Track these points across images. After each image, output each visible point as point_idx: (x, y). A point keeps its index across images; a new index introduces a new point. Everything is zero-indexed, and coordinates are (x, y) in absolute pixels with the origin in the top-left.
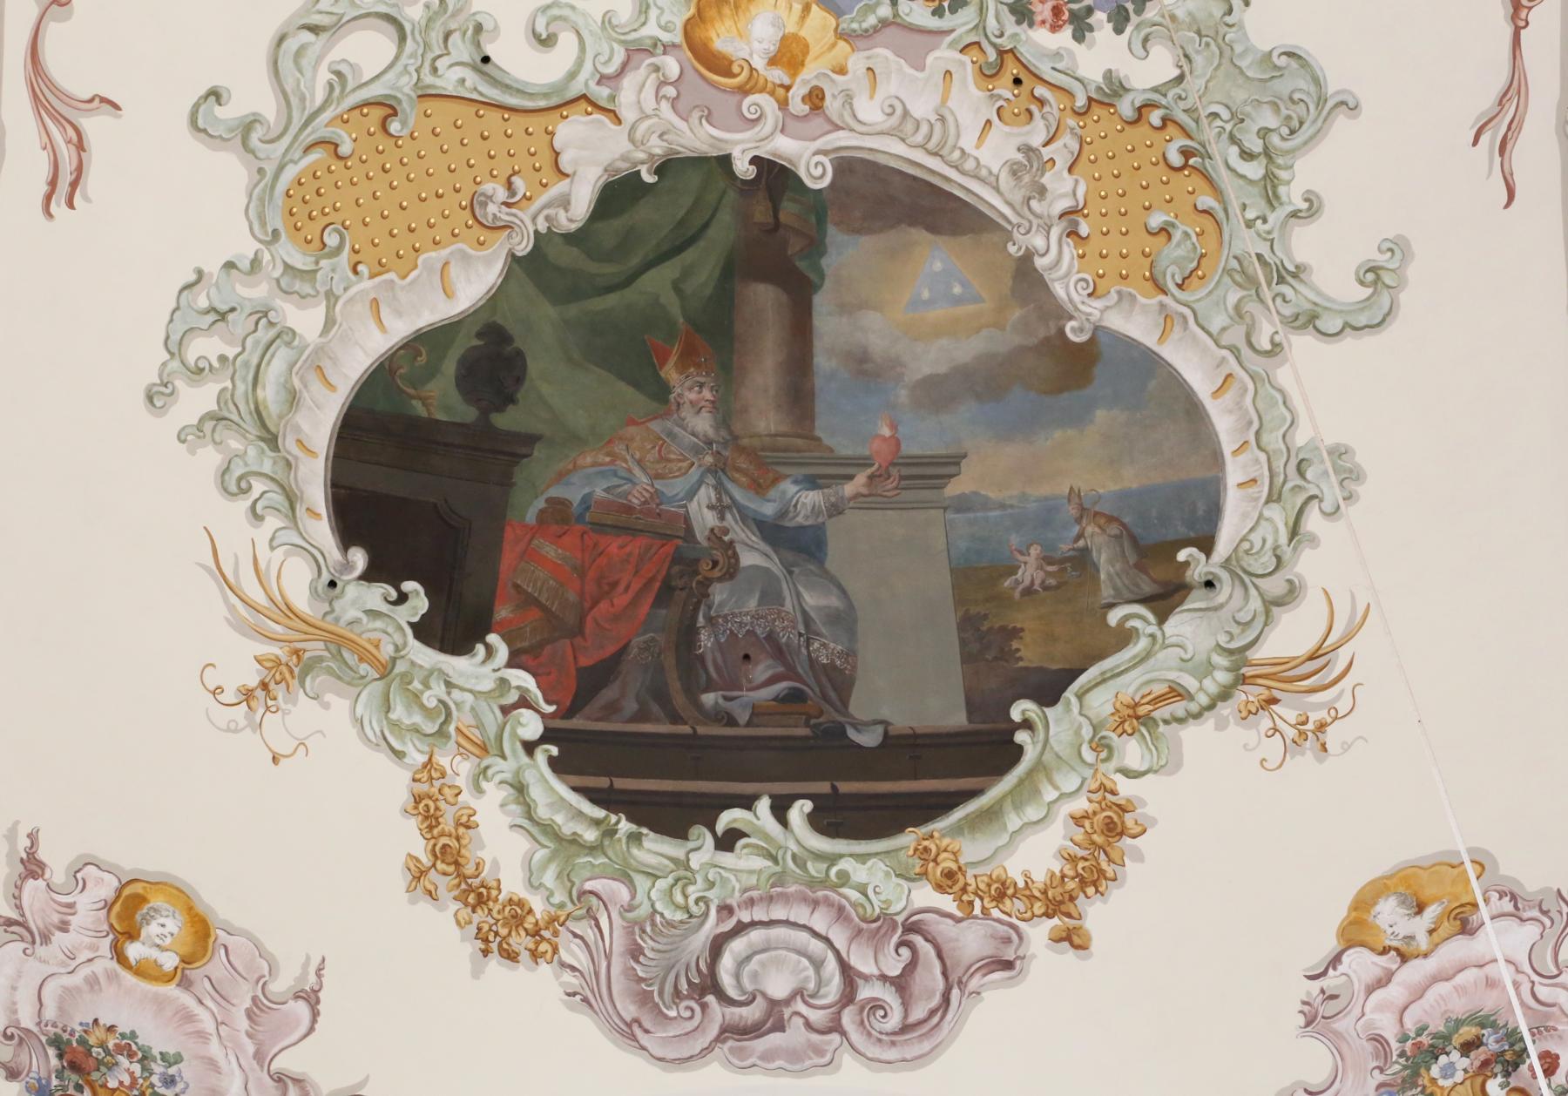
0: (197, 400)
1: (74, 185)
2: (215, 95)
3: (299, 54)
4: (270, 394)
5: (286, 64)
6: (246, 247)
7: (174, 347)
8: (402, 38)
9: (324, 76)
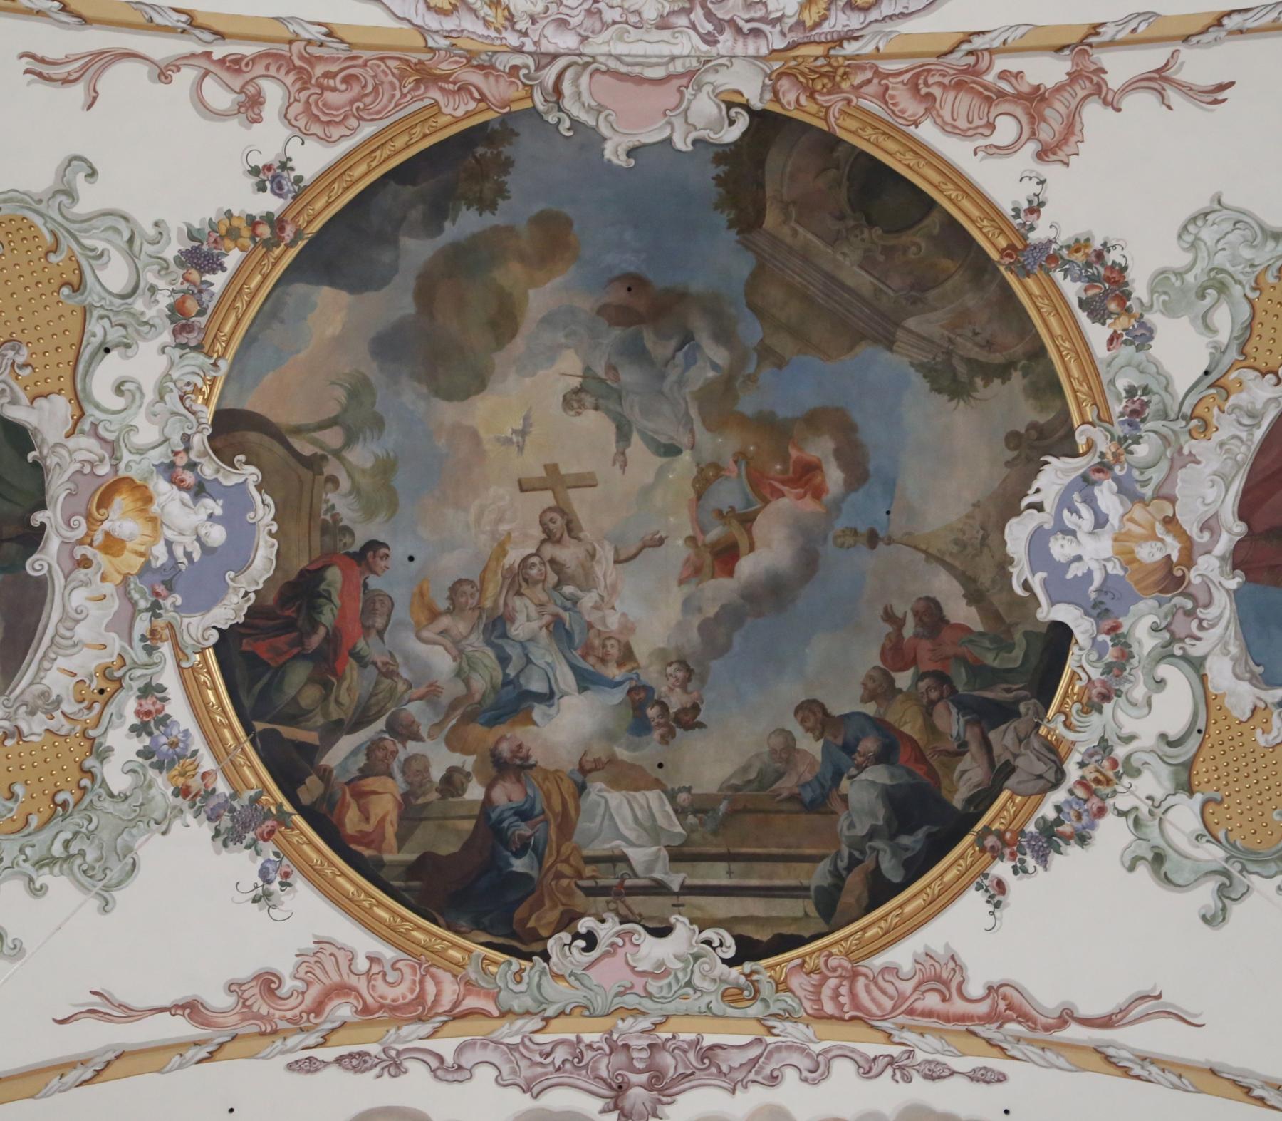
1: (40, 75)
2: (92, 173)
3: (117, 231)
5: (109, 221)
8: (123, 297)
9: (100, 245)
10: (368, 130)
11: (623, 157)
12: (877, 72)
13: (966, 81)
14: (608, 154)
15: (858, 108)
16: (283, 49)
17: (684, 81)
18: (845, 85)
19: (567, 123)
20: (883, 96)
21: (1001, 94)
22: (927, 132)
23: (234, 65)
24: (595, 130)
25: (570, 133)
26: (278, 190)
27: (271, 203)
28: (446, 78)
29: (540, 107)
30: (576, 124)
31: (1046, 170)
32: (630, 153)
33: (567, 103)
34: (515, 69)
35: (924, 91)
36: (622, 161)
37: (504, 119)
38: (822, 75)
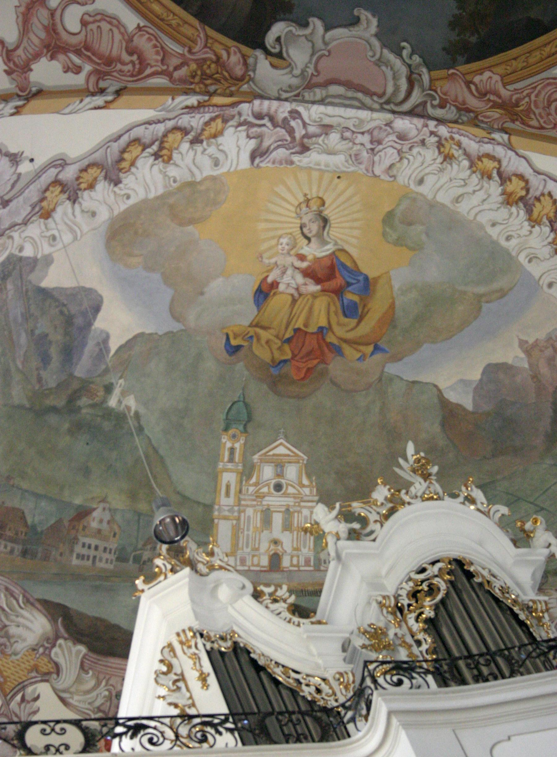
11: (363, 18)
14: (374, 22)
15: (183, 45)
17: (315, 80)
18: (194, 66)
19: (405, 53)
20: (165, 54)
24: (384, 45)
25: (404, 44)
28: (495, 105)
29: (425, 70)
30: (398, 52)
32: (356, 21)
33: (404, 71)
35: (135, 58)
36: (364, 14)
37: (453, 64)
38: (210, 77)
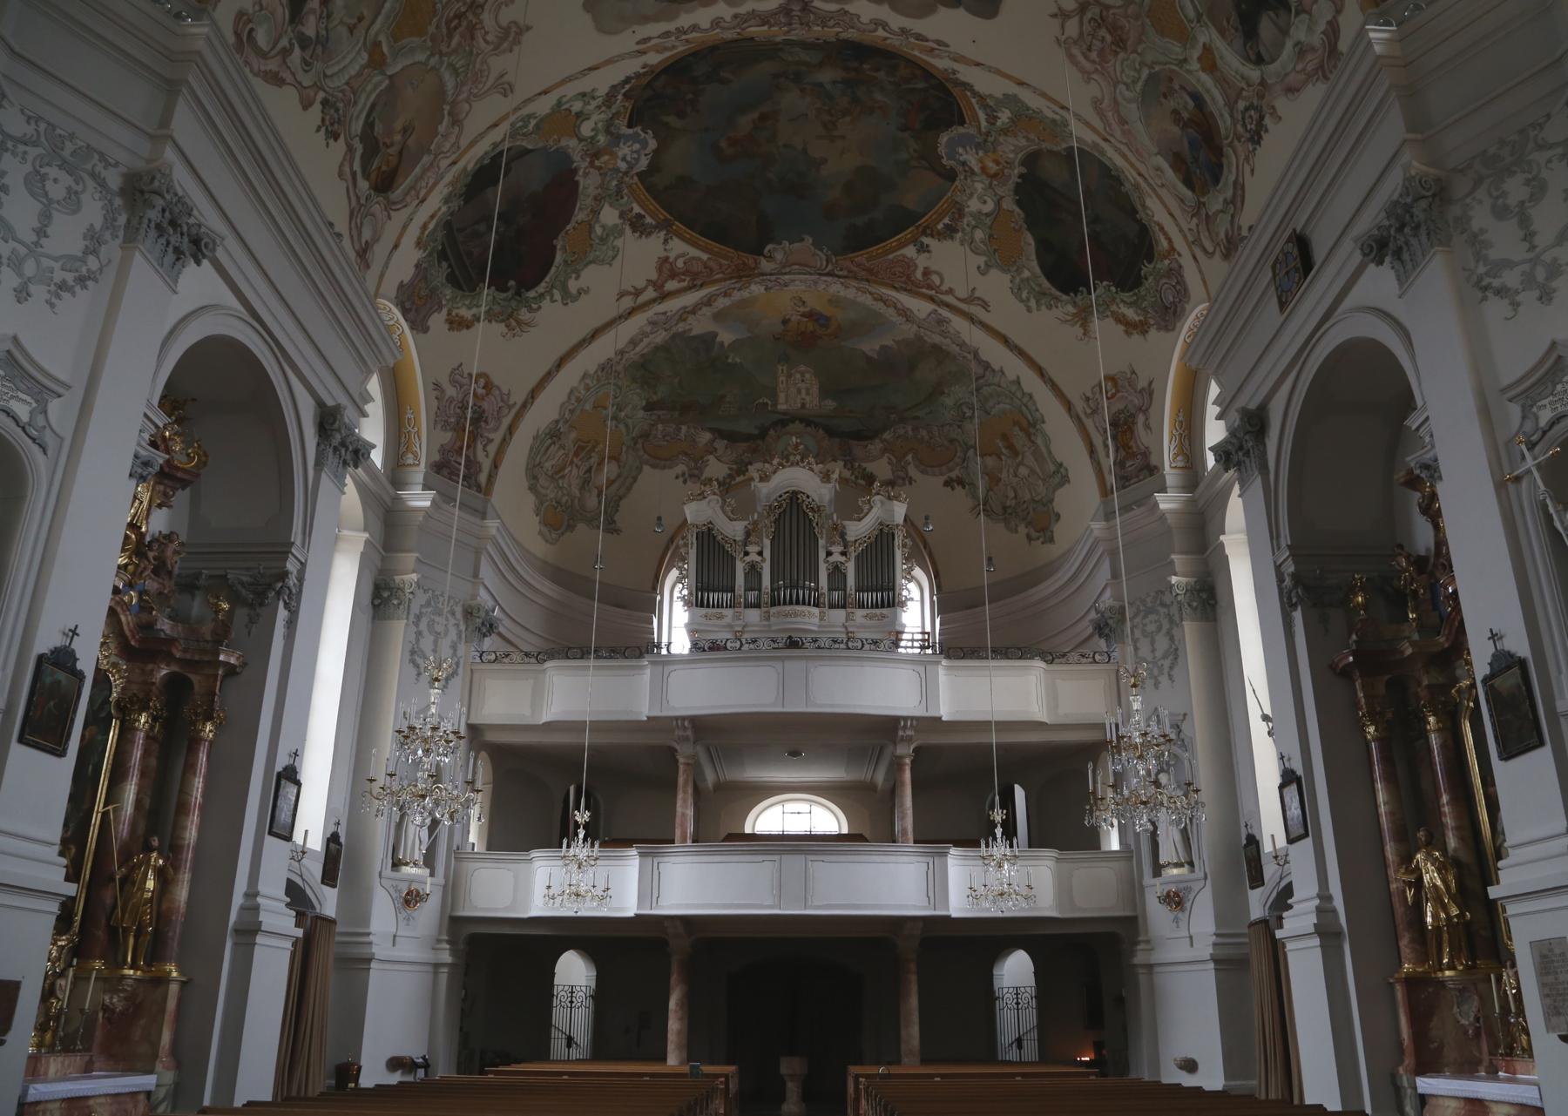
0: (1033, 303)
2: (979, 268)
4: (1037, 289)
6: (1008, 277)
7: (1022, 301)
10: (891, 257)
12: (723, 273)
13: (695, 276)
14: (811, 241)
16: (914, 288)
20: (721, 265)
21: (683, 274)
22: (705, 256)
23: (929, 287)
26: (922, 243)
27: (926, 240)
30: (821, 250)
31: (665, 254)
32: (803, 240)
33: (824, 257)
34: (841, 270)
